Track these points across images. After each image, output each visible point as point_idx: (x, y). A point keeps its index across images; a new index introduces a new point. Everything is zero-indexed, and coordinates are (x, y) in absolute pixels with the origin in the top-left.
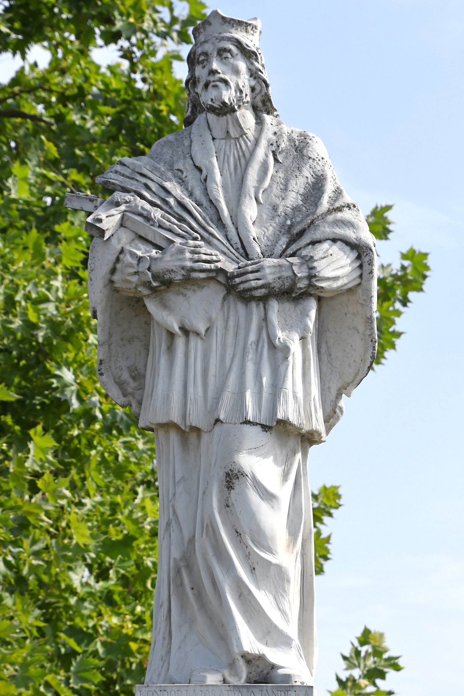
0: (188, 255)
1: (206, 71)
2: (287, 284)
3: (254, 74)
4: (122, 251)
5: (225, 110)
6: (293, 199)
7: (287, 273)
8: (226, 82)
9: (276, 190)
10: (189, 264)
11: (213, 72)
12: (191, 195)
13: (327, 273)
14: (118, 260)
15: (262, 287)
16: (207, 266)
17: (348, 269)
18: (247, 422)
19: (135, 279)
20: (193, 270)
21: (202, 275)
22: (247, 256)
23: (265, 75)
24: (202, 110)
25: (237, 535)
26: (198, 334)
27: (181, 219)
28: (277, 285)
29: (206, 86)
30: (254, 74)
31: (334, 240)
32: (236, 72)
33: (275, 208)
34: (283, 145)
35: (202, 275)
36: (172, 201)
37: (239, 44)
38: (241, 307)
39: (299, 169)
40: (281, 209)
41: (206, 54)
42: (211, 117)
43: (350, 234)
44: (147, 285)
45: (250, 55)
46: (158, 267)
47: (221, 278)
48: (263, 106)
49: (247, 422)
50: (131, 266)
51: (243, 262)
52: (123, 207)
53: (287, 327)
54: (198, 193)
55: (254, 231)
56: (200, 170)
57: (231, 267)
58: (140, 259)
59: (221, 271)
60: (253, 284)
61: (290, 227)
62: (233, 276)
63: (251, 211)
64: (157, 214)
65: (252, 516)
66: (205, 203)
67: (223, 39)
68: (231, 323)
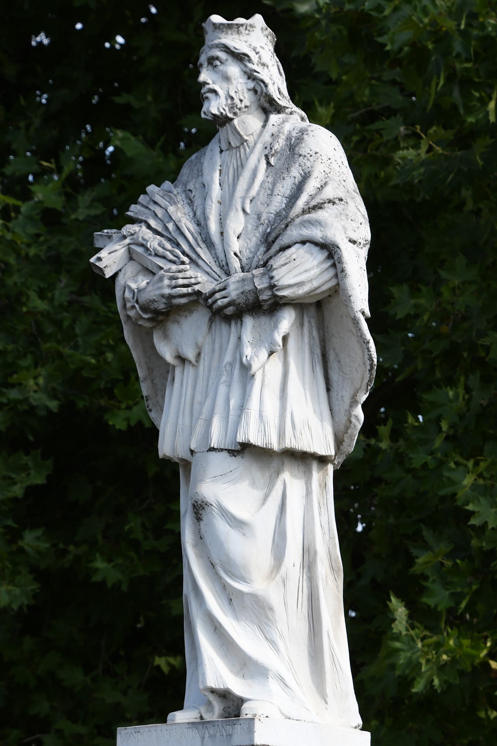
0: (166, 282)
2: (251, 298)
3: (250, 76)
5: (223, 121)
6: (278, 203)
7: (248, 287)
8: (214, 92)
9: (263, 198)
10: (167, 291)
13: (285, 281)
15: (229, 304)
16: (185, 290)
17: (316, 271)
18: (212, 449)
20: (171, 297)
21: (183, 301)
25: (211, 567)
26: (190, 362)
28: (242, 300)
30: (250, 76)
31: (303, 243)
32: (227, 78)
34: (277, 146)
35: (183, 301)
36: (170, 226)
37: (226, 49)
38: (224, 327)
39: (288, 170)
40: (264, 217)
43: (317, 234)
45: (240, 58)
49: (212, 449)
52: (127, 241)
53: (257, 344)
55: (235, 245)
60: (220, 303)
63: (237, 223)
65: (221, 546)
68: (217, 346)
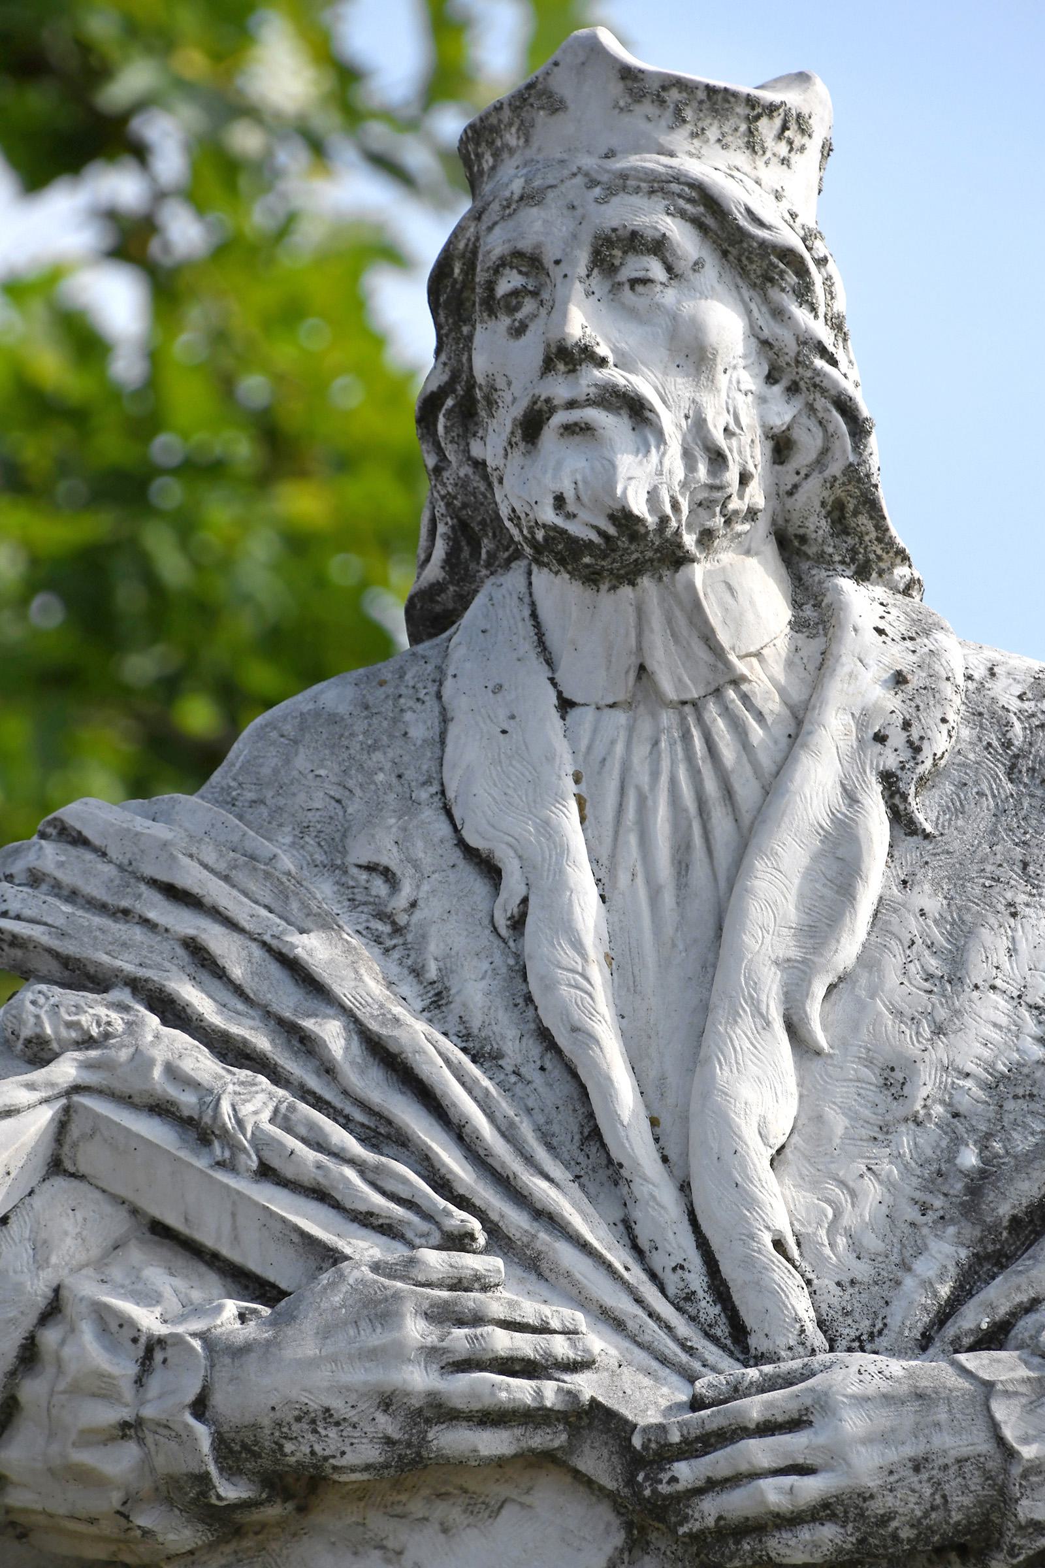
0: (416, 1330)
1: (528, 352)
3: (790, 367)
4: (54, 1309)
5: (630, 554)
8: (636, 409)
9: (899, 982)
10: (419, 1379)
11: (569, 357)
12: (437, 1002)
14: (29, 1355)
15: (823, 1511)
16: (521, 1390)
19: (119, 1463)
20: (440, 1412)
21: (493, 1443)
22: (738, 1338)
23: (849, 375)
24: (507, 554)
27: (382, 1134)
29: (531, 426)
32: (695, 356)
33: (894, 1080)
35: (493, 1443)
36: (332, 1034)
37: (708, 210)
40: (926, 1086)
41: (530, 262)
42: (554, 589)
44: (190, 1495)
45: (763, 266)
46: (249, 1398)
47: (595, 1461)
48: (833, 531)
50: (103, 1389)
51: (720, 1370)
52: (66, 1070)
54: (476, 993)
55: (778, 1204)
56: (491, 870)
57: (648, 1399)
58: (151, 1351)
59: (595, 1419)
60: (774, 1493)
61: (979, 1184)
62: (663, 1453)
63: (761, 1092)
64: (251, 1104)
66: (517, 1048)
67: (622, 183)
